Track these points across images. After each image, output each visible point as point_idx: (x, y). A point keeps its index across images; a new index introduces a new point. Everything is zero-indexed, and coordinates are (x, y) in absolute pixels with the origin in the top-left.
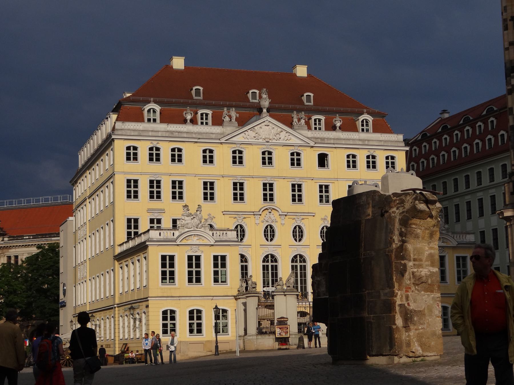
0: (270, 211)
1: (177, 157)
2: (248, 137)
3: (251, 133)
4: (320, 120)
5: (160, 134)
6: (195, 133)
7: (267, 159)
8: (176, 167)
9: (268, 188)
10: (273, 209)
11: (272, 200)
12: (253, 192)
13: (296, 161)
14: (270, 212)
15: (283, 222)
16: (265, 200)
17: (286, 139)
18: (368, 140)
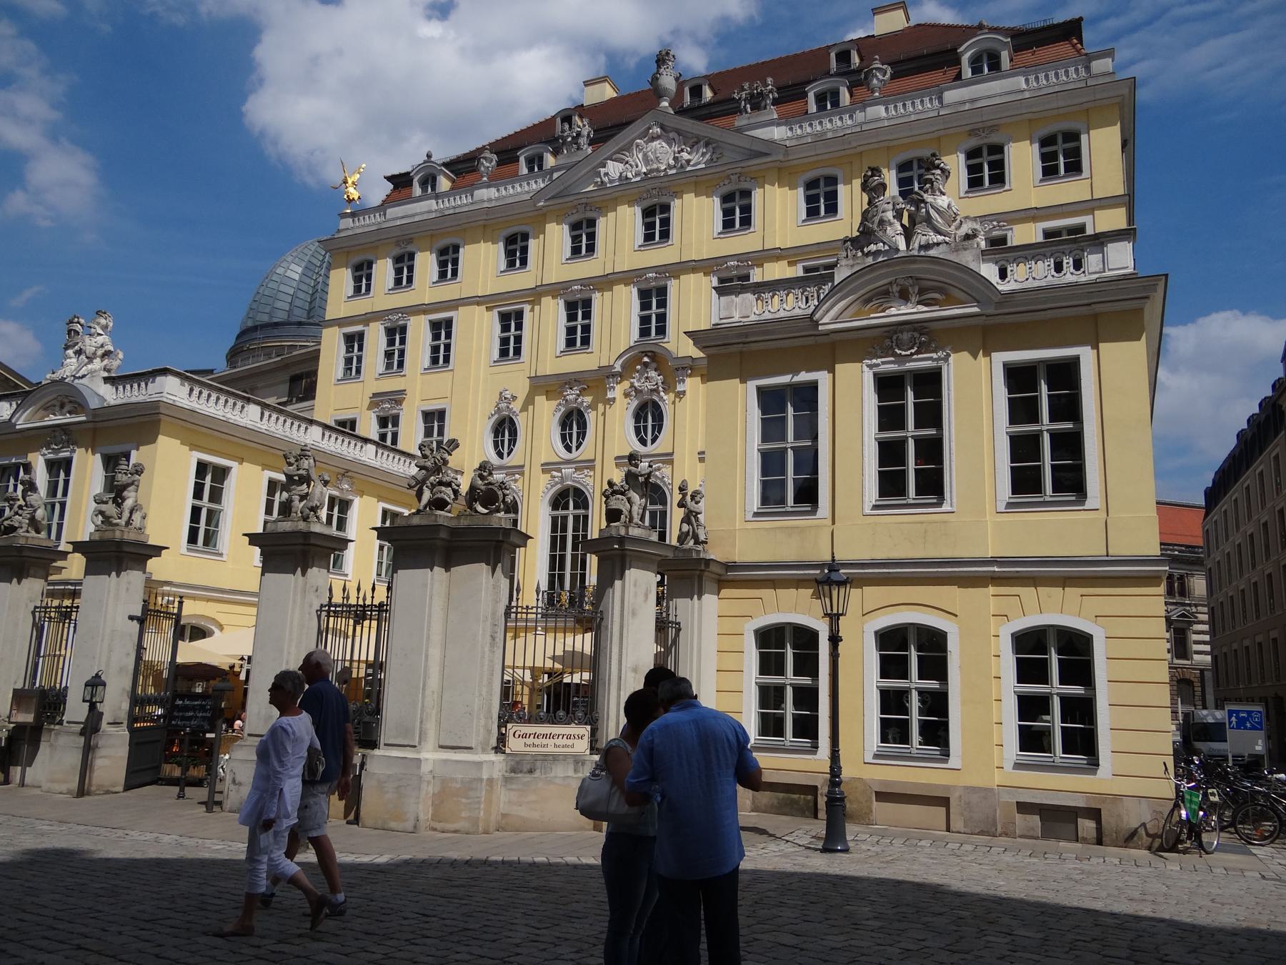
0: (646, 359)
1: (448, 263)
2: (606, 179)
3: (613, 169)
4: (835, 95)
5: (417, 219)
6: (490, 200)
7: (657, 225)
8: (449, 291)
9: (653, 296)
10: (654, 356)
11: (661, 331)
12: (617, 319)
13: (737, 213)
14: (646, 365)
15: (680, 388)
16: (644, 332)
17: (708, 156)
18: (973, 101)
